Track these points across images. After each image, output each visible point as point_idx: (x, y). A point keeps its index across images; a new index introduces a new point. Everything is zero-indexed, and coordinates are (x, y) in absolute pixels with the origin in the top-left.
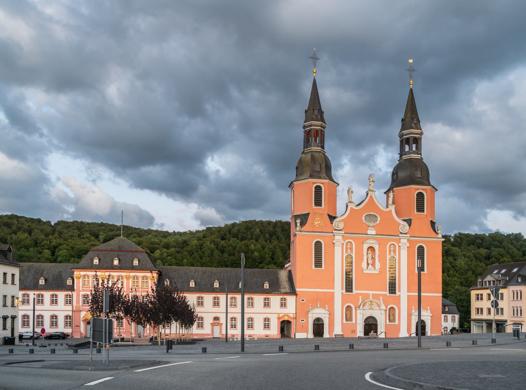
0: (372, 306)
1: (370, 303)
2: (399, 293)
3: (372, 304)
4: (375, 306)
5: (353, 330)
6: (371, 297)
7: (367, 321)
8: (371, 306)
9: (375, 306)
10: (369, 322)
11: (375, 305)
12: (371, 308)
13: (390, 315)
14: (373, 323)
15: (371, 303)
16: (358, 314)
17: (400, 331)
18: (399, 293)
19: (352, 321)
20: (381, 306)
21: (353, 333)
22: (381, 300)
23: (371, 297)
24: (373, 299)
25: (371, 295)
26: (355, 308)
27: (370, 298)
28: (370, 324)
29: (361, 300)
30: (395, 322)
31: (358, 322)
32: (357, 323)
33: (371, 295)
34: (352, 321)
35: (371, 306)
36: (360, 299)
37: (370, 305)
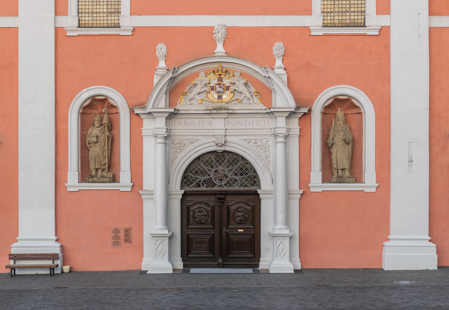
0: (226, 97)
1: (214, 82)
2: (383, 21)
3: (226, 82)
4: (242, 97)
5: (121, 228)
6: (220, 49)
7: (203, 178)
8: (220, 97)
9: (242, 97)
10: (210, 183)
11: (242, 88)
12: (218, 105)
13: (330, 142)
14: (236, 188)
15: (220, 79)
16: (145, 139)
17: (387, 230)
18: (383, 21)
19: (114, 179)
20: (275, 92)
21: (124, 245)
22: (279, 63)
23: (220, 49)
24: (228, 54)
25: (219, 35)
26: (132, 111)
27: (212, 55)
28: (214, 194)
29: (162, 64)
30: (358, 179)
31: (147, 184)
32: (142, 189)
33: (219, 35)
34: (114, 179)
35: (220, 97)
36: (157, 61)
37: (213, 88)
